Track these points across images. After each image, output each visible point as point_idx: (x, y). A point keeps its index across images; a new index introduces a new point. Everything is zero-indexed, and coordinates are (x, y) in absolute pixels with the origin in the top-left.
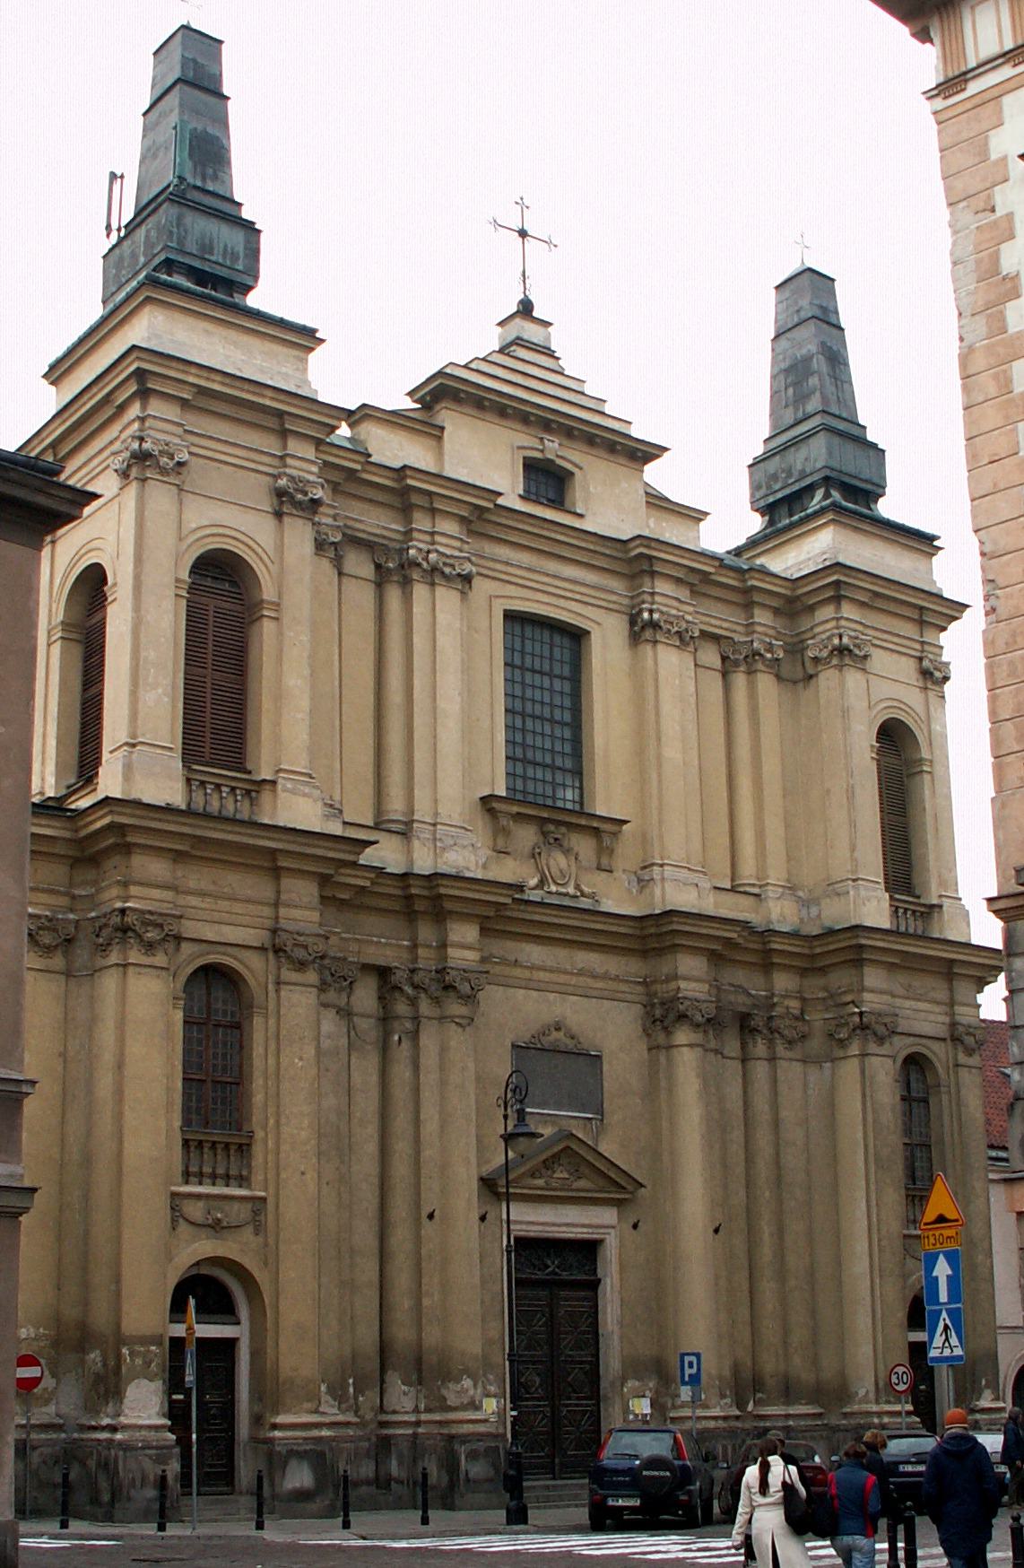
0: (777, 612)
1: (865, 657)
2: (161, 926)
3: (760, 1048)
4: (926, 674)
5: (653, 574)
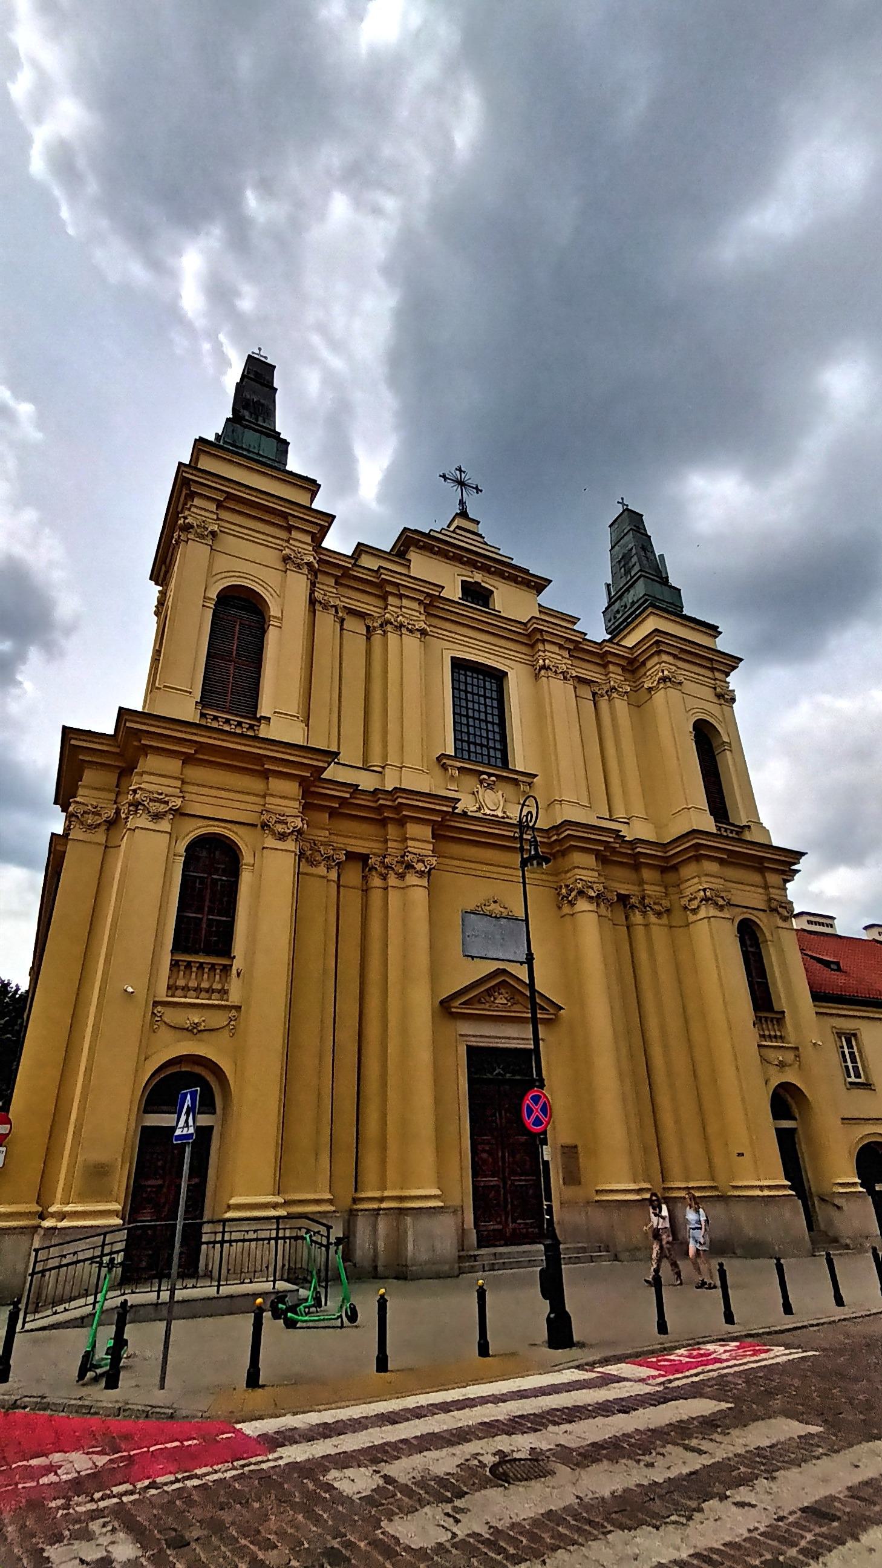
0: (624, 668)
1: (680, 683)
2: (167, 803)
3: (637, 918)
4: (719, 696)
5: (544, 641)
